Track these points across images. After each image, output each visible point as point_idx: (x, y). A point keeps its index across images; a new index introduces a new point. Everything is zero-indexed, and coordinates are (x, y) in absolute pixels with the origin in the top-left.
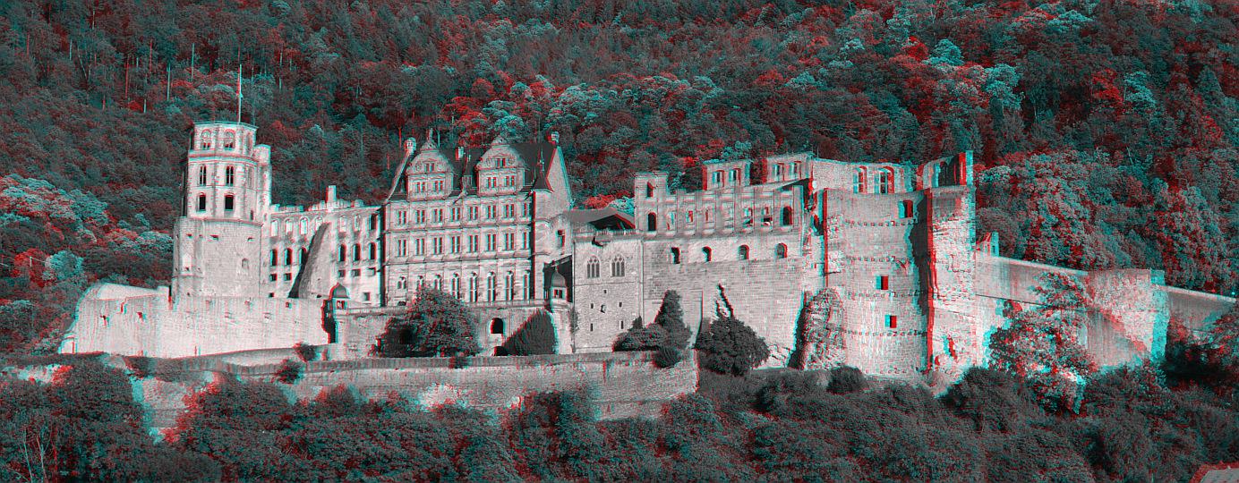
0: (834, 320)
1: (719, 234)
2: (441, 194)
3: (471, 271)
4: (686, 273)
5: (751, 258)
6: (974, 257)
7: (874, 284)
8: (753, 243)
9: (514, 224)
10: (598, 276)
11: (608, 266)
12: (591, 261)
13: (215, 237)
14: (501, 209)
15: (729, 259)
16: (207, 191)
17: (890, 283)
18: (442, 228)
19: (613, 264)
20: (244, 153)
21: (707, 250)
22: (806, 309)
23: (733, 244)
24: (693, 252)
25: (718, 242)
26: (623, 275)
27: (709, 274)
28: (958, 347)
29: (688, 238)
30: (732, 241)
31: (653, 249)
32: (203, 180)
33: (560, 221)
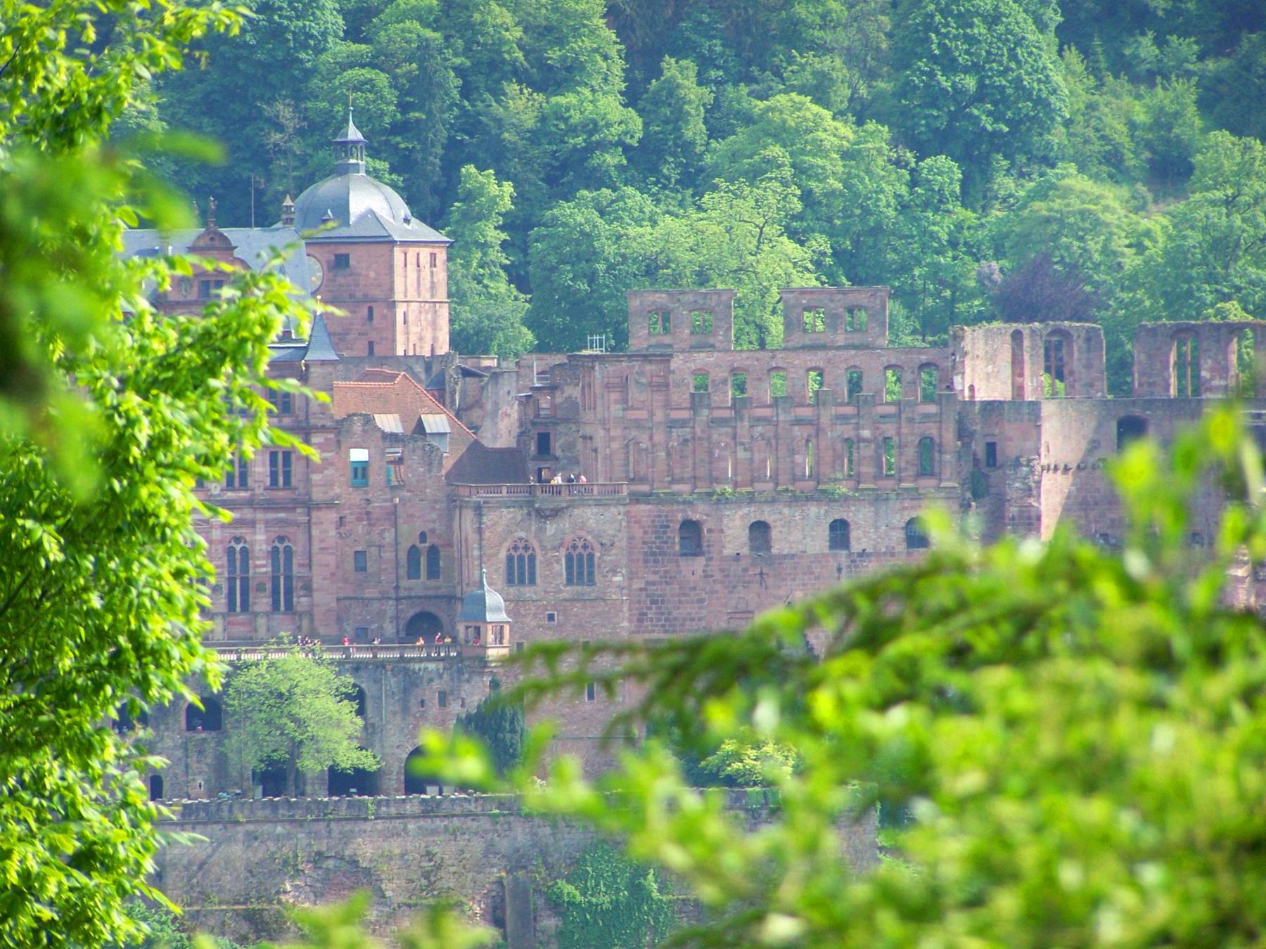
4: (718, 576)
5: (856, 547)
8: (860, 518)
10: (532, 581)
11: (558, 561)
12: (516, 548)
15: (810, 551)
19: (569, 558)
21: (760, 530)
23: (818, 517)
24: (732, 530)
25: (786, 511)
26: (591, 582)
27: (770, 581)
29: (722, 500)
30: (813, 510)
31: (646, 521)
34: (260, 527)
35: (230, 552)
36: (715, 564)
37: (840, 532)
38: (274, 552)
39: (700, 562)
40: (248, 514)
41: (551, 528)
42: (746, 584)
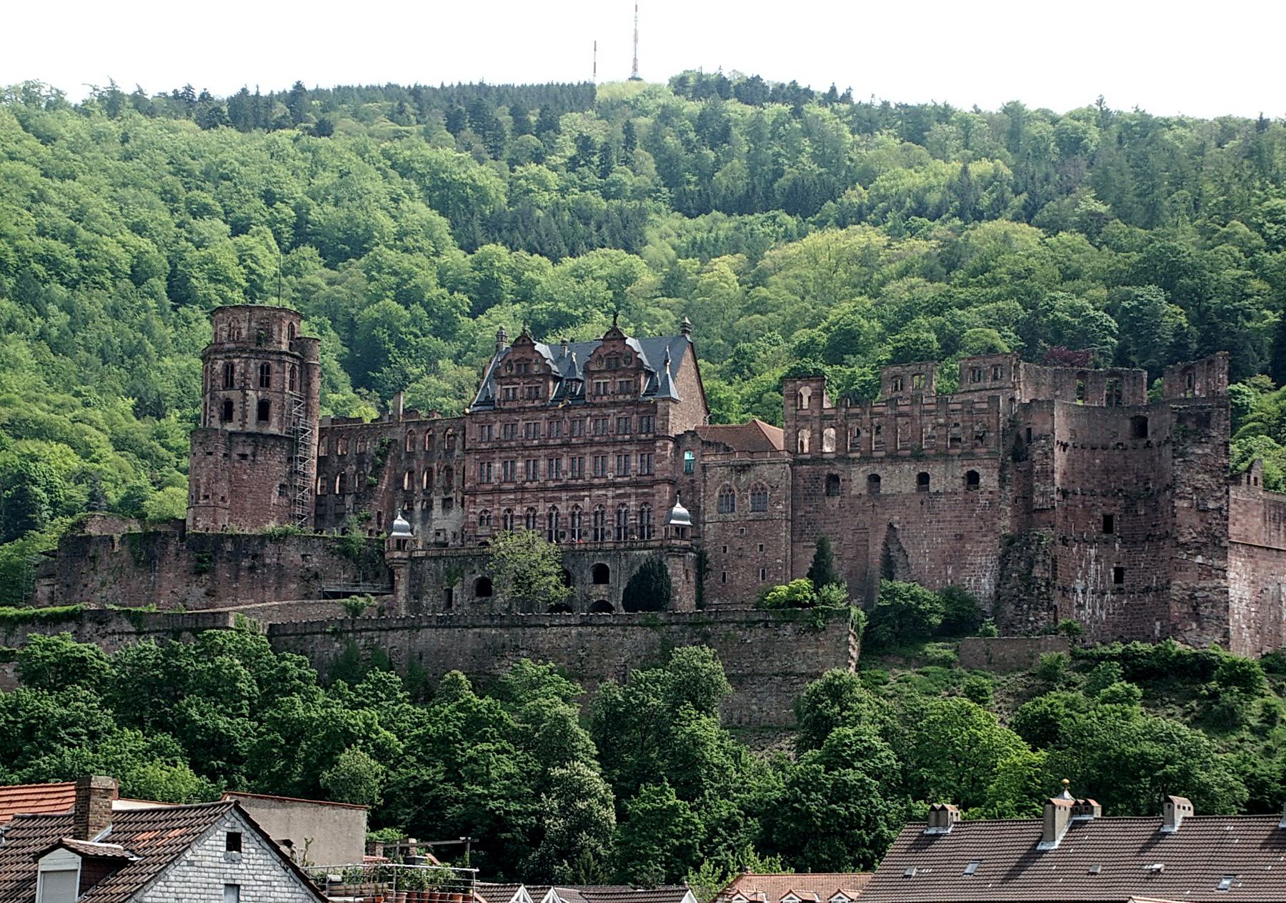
0: (1037, 572)
1: (894, 458)
2: (537, 403)
3: (572, 503)
4: (847, 507)
5: (932, 489)
6: (1227, 492)
7: (1094, 528)
9: (630, 442)
10: (733, 511)
13: (244, 456)
14: (611, 421)
16: (235, 395)
17: (1116, 527)
18: (537, 447)
19: (753, 494)
20: (284, 348)
21: (875, 479)
22: (1003, 560)
24: (857, 479)
25: (889, 468)
27: (878, 510)
28: (1205, 611)
31: (807, 476)
32: (229, 384)
33: (689, 438)
34: (633, 497)
35: (619, 513)
36: (846, 501)
37: (923, 479)
38: (642, 512)
39: (838, 498)
40: (628, 490)
41: (743, 478)
42: (864, 512)
